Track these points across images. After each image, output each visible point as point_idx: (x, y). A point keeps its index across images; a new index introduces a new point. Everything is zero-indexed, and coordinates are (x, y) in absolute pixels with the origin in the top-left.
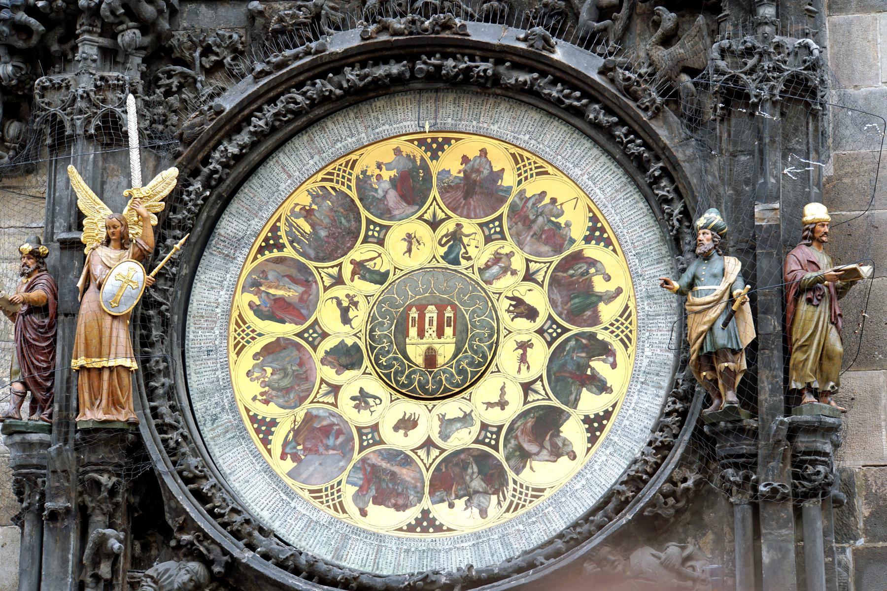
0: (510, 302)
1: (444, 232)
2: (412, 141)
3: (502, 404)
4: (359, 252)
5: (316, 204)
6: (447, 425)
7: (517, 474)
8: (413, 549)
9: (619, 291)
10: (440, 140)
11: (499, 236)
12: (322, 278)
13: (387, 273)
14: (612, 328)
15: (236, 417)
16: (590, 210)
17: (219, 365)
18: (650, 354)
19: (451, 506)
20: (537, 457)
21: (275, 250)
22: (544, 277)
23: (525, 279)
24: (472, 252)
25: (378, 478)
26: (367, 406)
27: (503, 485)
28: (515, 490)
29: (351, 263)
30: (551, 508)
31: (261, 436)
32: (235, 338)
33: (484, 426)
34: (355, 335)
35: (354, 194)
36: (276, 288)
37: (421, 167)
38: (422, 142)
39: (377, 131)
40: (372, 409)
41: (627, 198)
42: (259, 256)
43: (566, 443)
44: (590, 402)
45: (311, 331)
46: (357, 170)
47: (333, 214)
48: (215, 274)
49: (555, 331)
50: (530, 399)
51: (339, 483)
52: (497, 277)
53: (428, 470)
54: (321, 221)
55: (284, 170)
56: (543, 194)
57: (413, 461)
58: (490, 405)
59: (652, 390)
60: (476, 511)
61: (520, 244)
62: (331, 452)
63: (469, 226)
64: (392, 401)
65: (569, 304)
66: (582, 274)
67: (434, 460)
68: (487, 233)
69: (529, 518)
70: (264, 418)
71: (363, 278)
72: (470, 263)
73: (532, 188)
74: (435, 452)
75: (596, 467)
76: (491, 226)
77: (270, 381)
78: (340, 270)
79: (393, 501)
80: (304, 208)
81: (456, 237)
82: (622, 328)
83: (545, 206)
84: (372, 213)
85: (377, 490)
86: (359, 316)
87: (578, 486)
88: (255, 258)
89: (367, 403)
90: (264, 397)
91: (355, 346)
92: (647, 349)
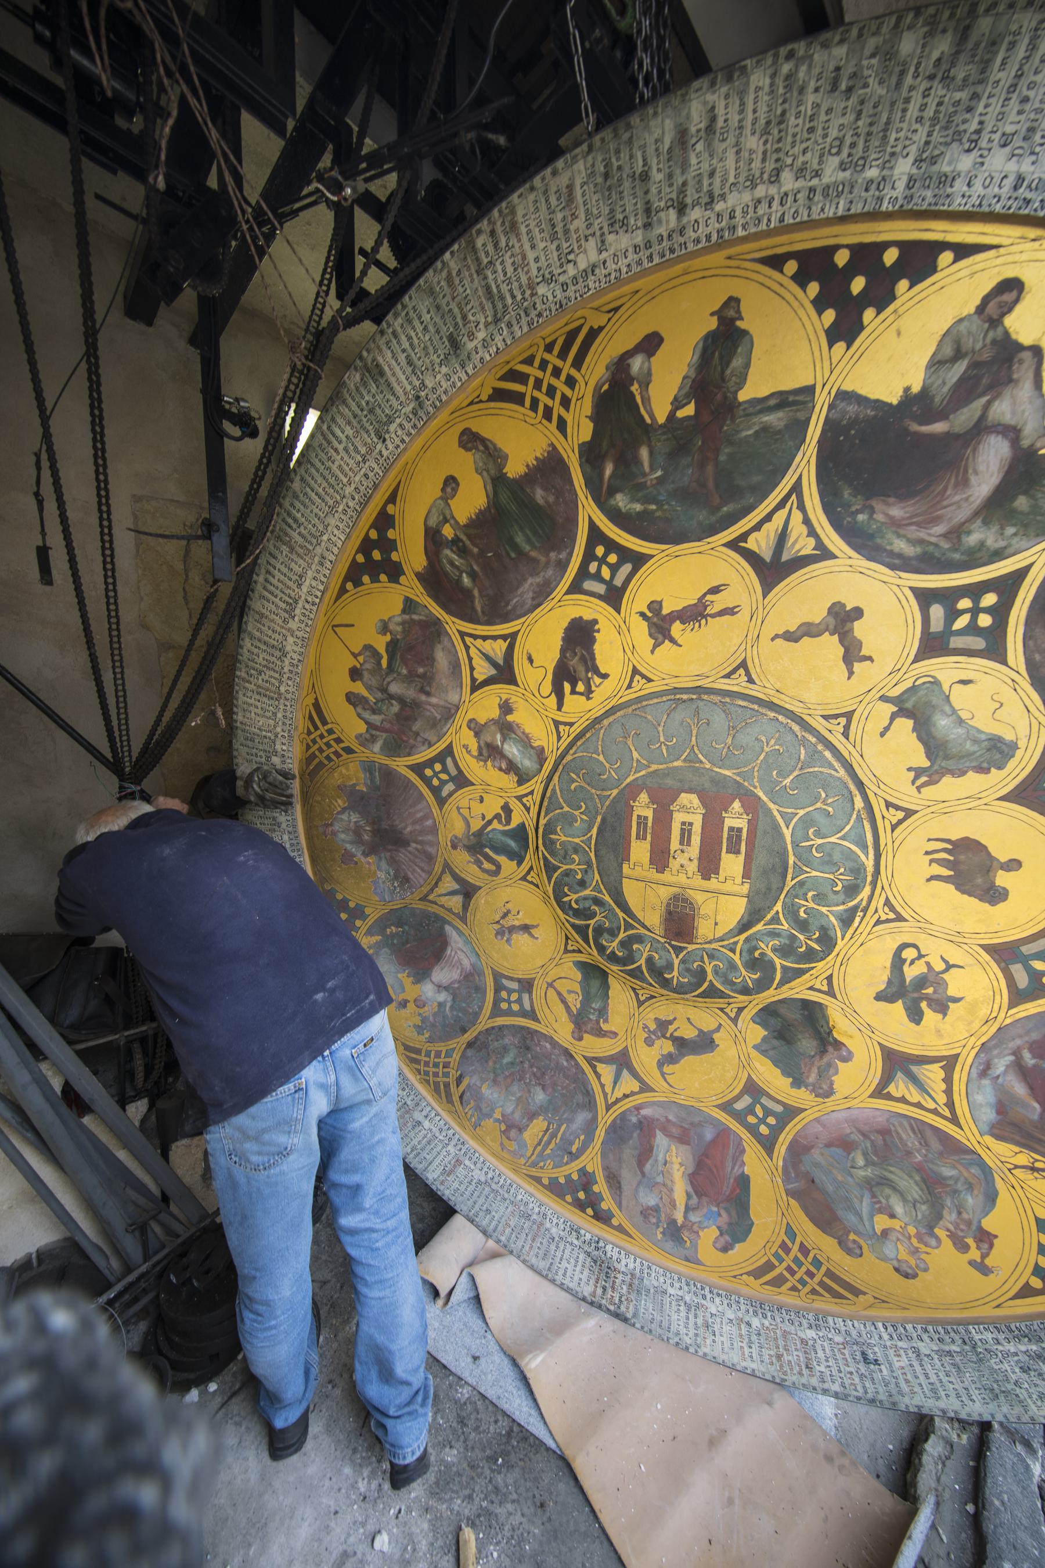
4: (556, 1026)
5: (493, 1110)
9: (470, 440)
11: (449, 761)
14: (558, 410)
18: (591, 245)
22: (495, 638)
23: (512, 680)
24: (493, 806)
26: (930, 979)
29: (580, 1039)
33: (933, 645)
34: (735, 1021)
36: (671, 1190)
37: (382, 932)
40: (939, 966)
41: (295, 520)
43: (948, 351)
45: (751, 1119)
47: (500, 1079)
48: (674, 1317)
49: (603, 561)
50: (807, 547)
52: (525, 741)
54: (519, 1099)
59: (698, 160)
61: (450, 713)
65: (533, 554)
66: (463, 552)
68: (450, 787)
71: (603, 1012)
72: (515, 804)
76: (435, 782)
81: (478, 844)
82: (548, 379)
83: (369, 688)
84: (481, 1008)
89: (921, 982)
90: (970, 1241)
92: (582, 265)
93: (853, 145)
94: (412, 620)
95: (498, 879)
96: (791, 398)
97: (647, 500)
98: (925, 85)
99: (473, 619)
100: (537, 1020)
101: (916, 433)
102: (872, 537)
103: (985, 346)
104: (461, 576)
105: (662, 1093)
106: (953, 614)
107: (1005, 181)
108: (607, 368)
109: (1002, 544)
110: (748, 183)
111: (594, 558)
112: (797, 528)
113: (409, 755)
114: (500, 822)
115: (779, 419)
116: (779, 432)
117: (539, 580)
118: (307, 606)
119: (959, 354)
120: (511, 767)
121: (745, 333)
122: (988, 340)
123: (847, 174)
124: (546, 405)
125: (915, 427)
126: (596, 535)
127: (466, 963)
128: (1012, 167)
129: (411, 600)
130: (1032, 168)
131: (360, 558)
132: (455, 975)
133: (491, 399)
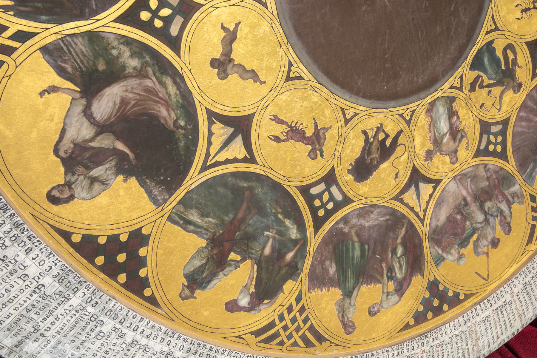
0: (392, 135)
1: (520, 60)
7: (44, 50)
9: (348, 327)
11: (482, 147)
14: (296, 308)
20: (79, 108)
43: (97, 187)
44: (173, 250)
50: (217, 127)
58: (230, 37)
61: (461, 178)
65: (356, 239)
66: (391, 269)
68: (494, 129)
72: (466, 87)
76: (500, 139)
81: (506, 77)
82: (292, 328)
83: (494, 228)
93: (92, 330)
94: (443, 250)
96: (181, 222)
97: (281, 223)
98: (47, 334)
99: (411, 225)
101: (132, 152)
102: (183, 107)
103: (79, 175)
104: (401, 256)
106: (168, 21)
107: (34, 257)
108: (260, 310)
109: (123, 47)
110: (147, 350)
111: (326, 211)
112: (217, 142)
113: (502, 169)
114: (483, 81)
115: (193, 215)
116: (197, 208)
117: (362, 221)
118: (493, 302)
119: (93, 180)
120: (452, 114)
121: (186, 276)
122: (76, 177)
123: (102, 318)
124: (301, 315)
125: (131, 156)
126: (318, 223)
128: (28, 262)
129: (435, 263)
130: (20, 253)
131: (445, 307)
133: (326, 340)
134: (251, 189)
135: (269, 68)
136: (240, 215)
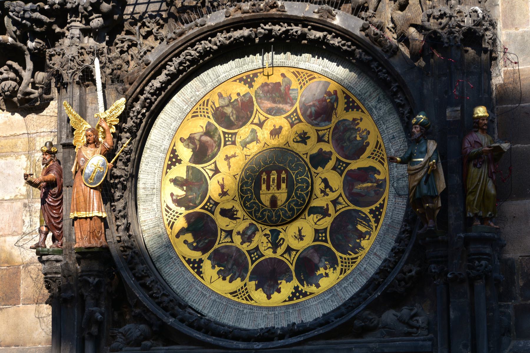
1: (283, 247)
2: (311, 294)
3: (227, 158)
6: (255, 139)
7: (209, 122)
8: (250, 64)
9: (178, 236)
10: (295, 299)
12: (344, 201)
13: (309, 215)
14: (178, 215)
15: (366, 105)
16: (202, 278)
17: (386, 132)
19: (238, 94)
21: (374, 209)
22: (221, 235)
24: (265, 240)
25: (282, 98)
26: (300, 136)
27: (214, 114)
28: (207, 113)
30: (185, 108)
31: (351, 100)
32: (382, 150)
33: (234, 143)
34: (318, 174)
35: (338, 254)
36: (368, 187)
38: (305, 295)
39: (331, 294)
42: (382, 202)
44: (180, 171)
45: (342, 168)
46: (338, 269)
50: (213, 165)
51: (301, 87)
52: (247, 229)
53: (257, 110)
55: (379, 257)
56: (231, 281)
57: (267, 113)
58: (234, 156)
60: (224, 95)
61: (238, 250)
62: (311, 103)
63: (269, 254)
64: (288, 142)
66: (200, 241)
67: (255, 116)
68: (258, 252)
69: (195, 100)
70: (352, 110)
71: (322, 208)
72: (264, 233)
73: (238, 283)
74: (256, 121)
75: (167, 137)
77: (356, 132)
78: (335, 208)
79: (270, 87)
80: (364, 238)
81: (275, 246)
82: (172, 216)
85: (280, 90)
86: (319, 186)
87: (174, 124)
88: (384, 200)
89: (300, 137)
91: (316, 169)
92: (155, 207)
95: (286, 239)
97: (198, 197)
100: (327, 228)
105: (341, 191)
106: (229, 141)
117: (210, 222)
119: (188, 145)
127: (312, 251)
132: (316, 255)
134: (203, 182)
135: (233, 169)
136: (196, 184)
